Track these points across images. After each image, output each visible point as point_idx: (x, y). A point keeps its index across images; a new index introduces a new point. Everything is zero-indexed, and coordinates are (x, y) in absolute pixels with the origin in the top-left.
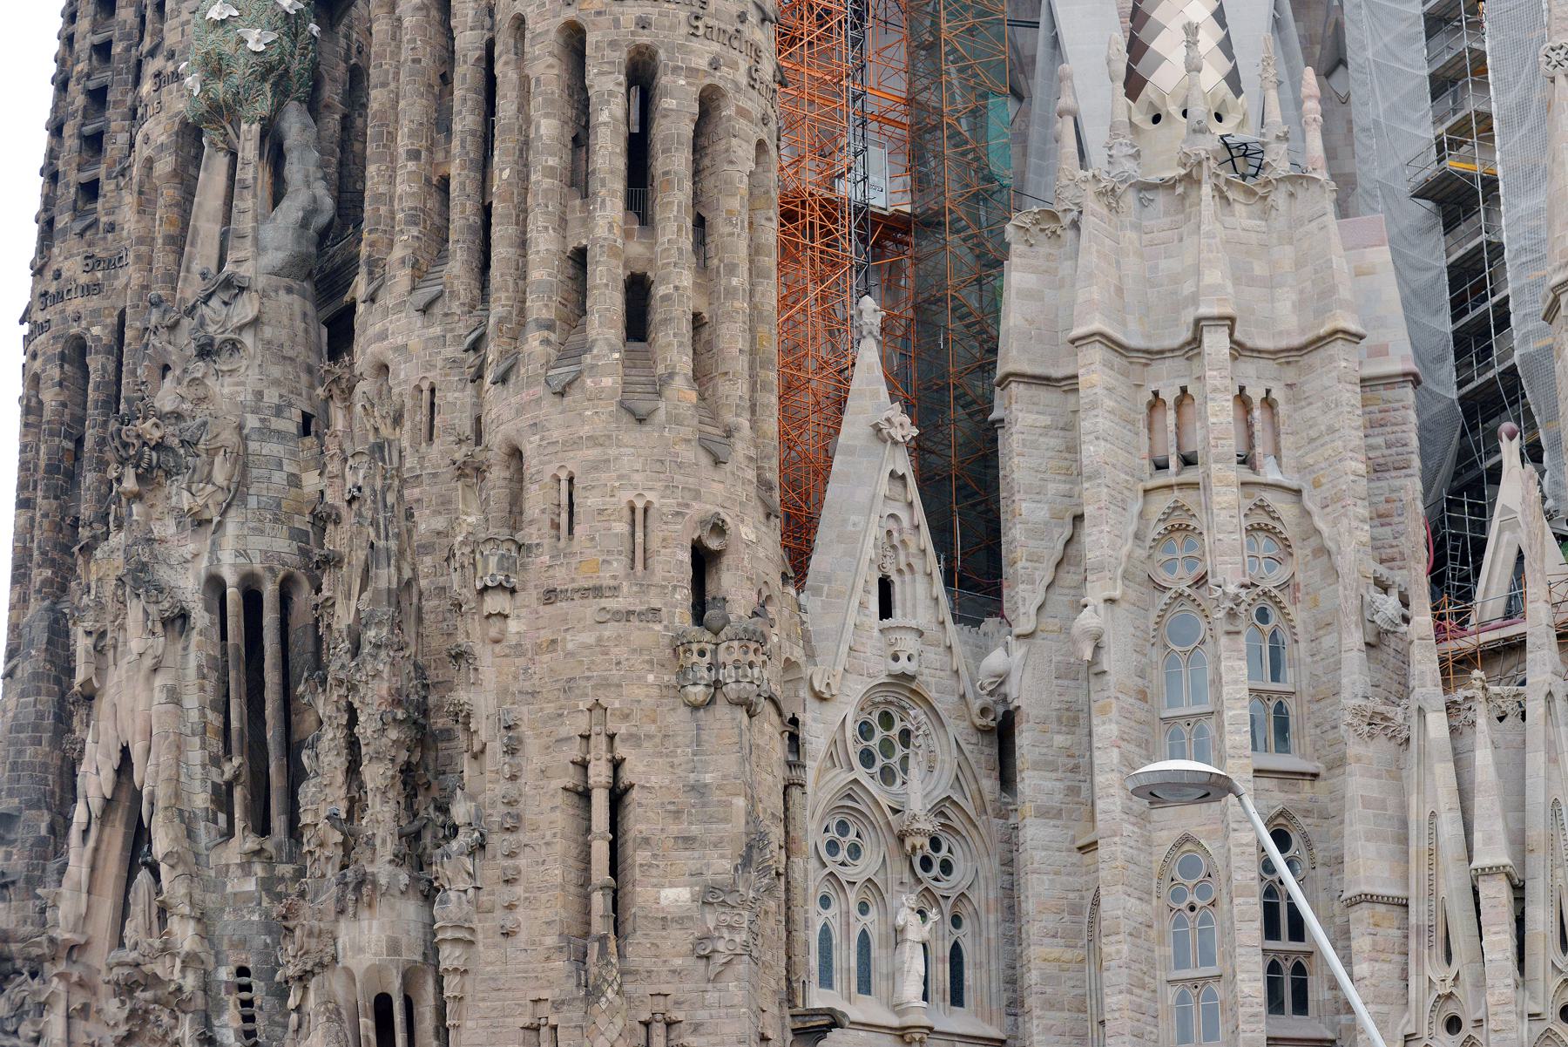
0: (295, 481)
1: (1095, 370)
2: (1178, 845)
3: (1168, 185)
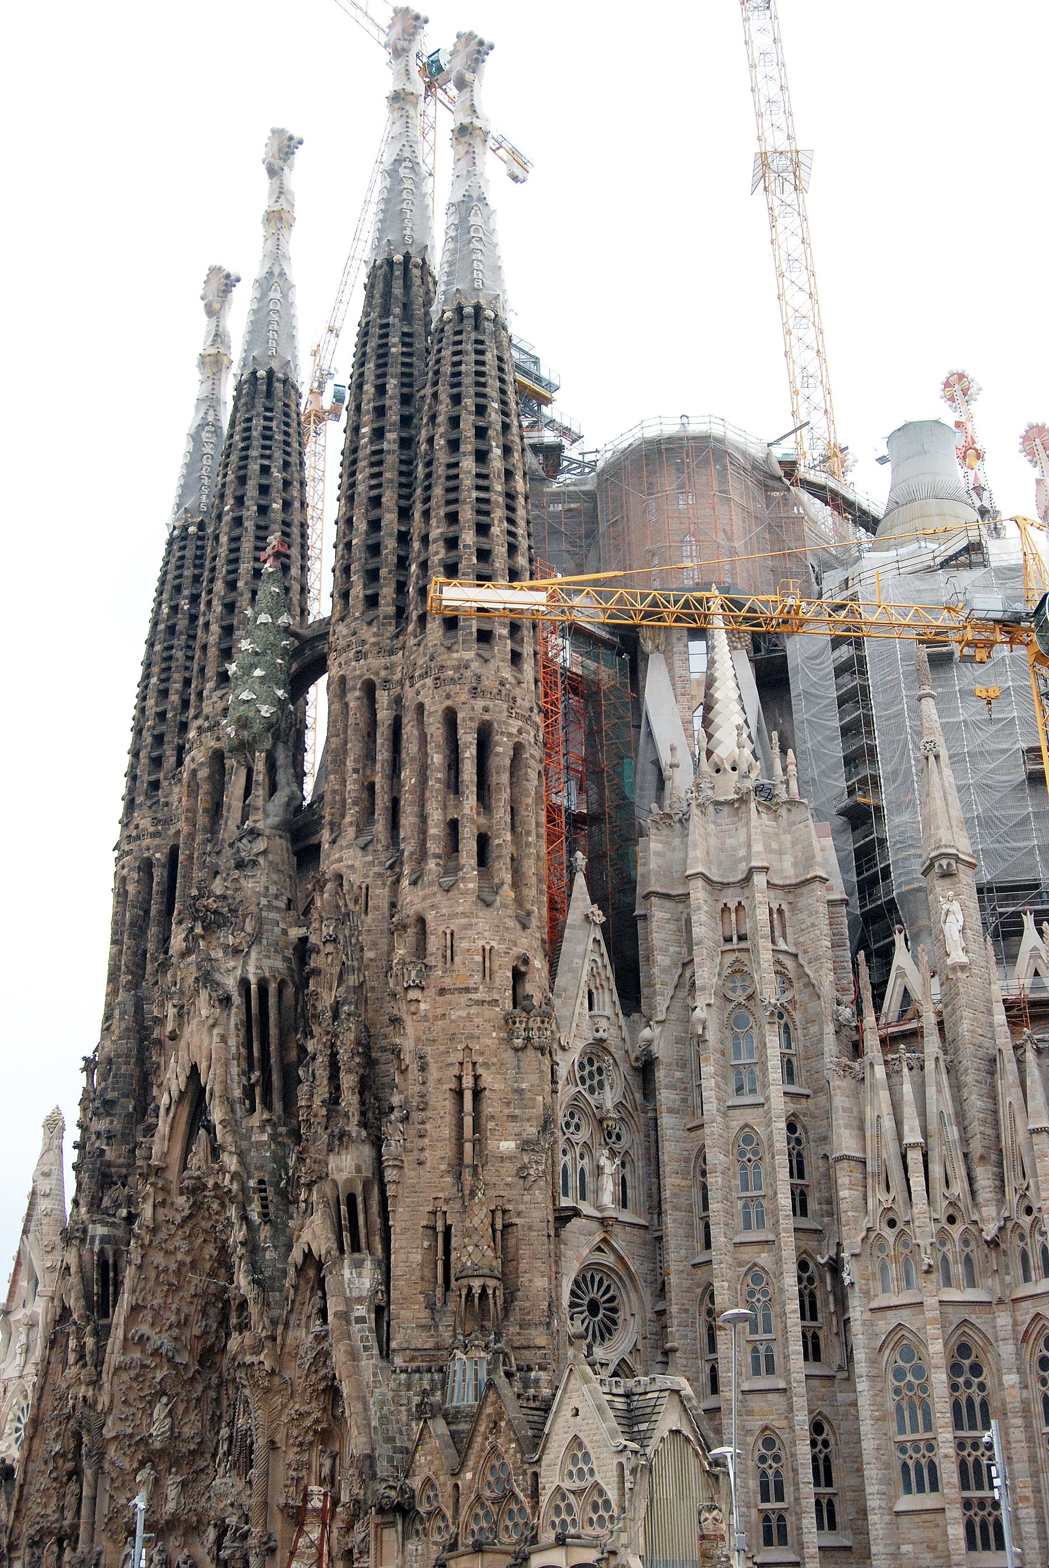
0: (285, 932)
1: (698, 893)
2: (742, 1128)
3: (730, 803)
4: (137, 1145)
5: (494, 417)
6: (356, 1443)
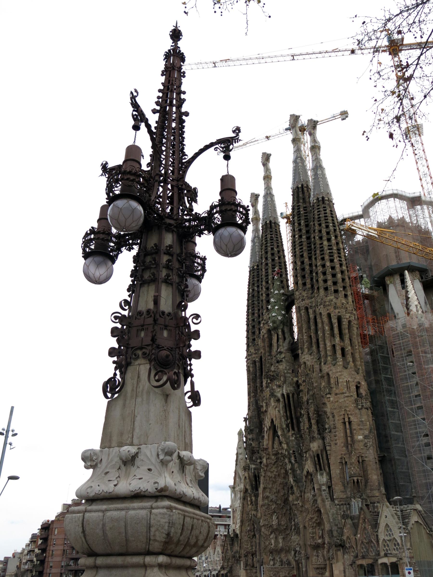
0: (292, 379)
4: (260, 442)
5: (331, 228)
6: (327, 527)
